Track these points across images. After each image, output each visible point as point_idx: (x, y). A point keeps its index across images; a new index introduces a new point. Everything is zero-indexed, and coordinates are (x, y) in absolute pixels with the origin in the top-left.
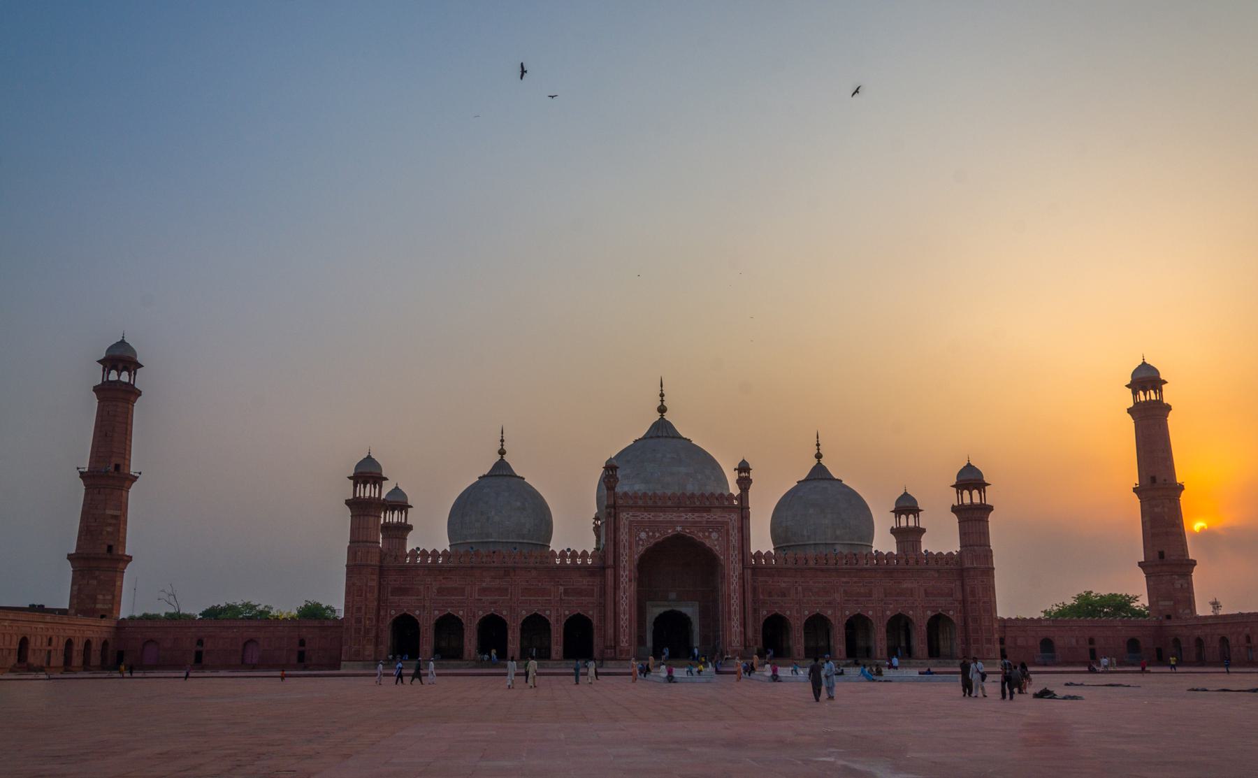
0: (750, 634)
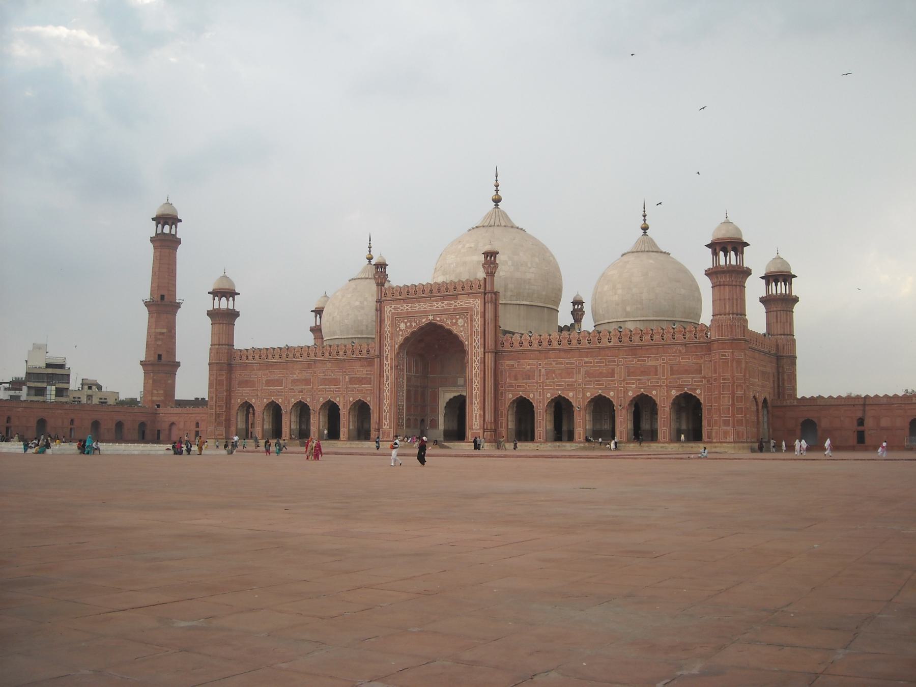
0: (489, 417)
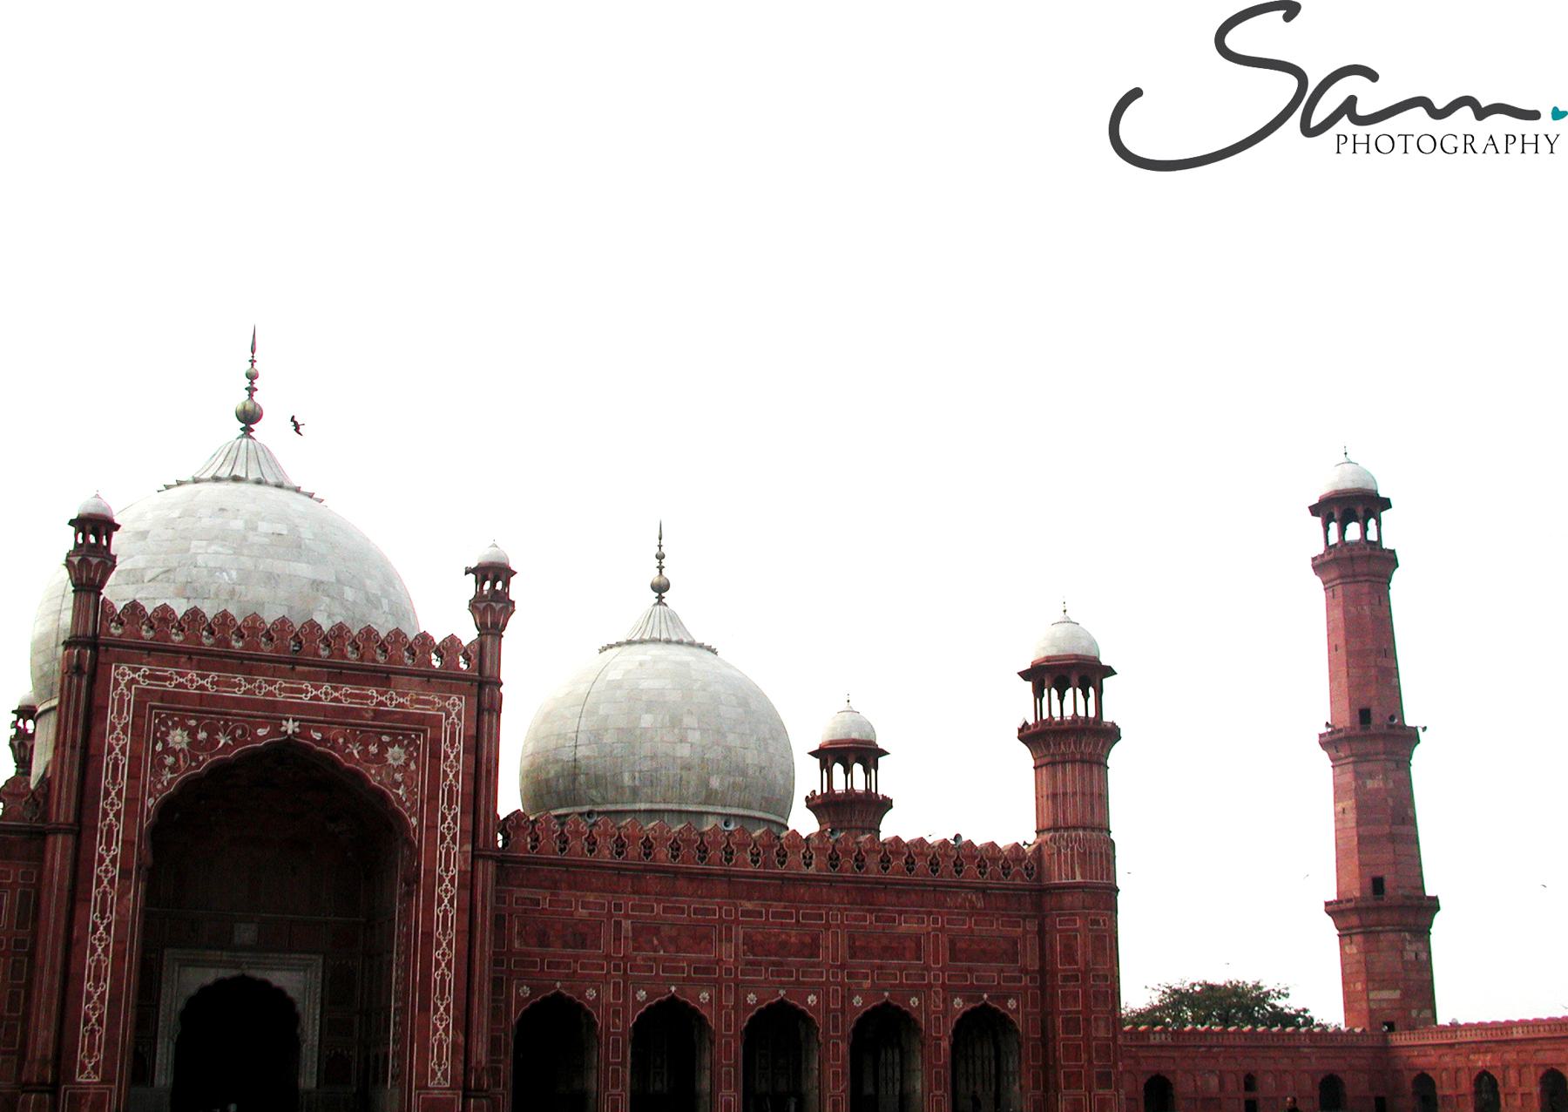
0: (481, 1052)
